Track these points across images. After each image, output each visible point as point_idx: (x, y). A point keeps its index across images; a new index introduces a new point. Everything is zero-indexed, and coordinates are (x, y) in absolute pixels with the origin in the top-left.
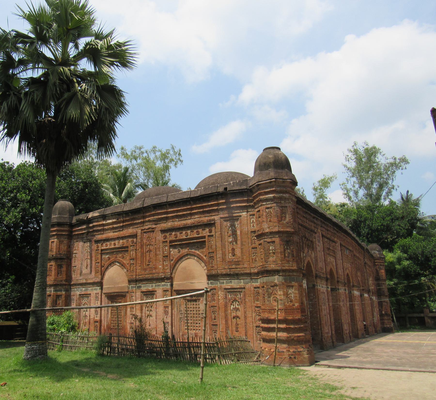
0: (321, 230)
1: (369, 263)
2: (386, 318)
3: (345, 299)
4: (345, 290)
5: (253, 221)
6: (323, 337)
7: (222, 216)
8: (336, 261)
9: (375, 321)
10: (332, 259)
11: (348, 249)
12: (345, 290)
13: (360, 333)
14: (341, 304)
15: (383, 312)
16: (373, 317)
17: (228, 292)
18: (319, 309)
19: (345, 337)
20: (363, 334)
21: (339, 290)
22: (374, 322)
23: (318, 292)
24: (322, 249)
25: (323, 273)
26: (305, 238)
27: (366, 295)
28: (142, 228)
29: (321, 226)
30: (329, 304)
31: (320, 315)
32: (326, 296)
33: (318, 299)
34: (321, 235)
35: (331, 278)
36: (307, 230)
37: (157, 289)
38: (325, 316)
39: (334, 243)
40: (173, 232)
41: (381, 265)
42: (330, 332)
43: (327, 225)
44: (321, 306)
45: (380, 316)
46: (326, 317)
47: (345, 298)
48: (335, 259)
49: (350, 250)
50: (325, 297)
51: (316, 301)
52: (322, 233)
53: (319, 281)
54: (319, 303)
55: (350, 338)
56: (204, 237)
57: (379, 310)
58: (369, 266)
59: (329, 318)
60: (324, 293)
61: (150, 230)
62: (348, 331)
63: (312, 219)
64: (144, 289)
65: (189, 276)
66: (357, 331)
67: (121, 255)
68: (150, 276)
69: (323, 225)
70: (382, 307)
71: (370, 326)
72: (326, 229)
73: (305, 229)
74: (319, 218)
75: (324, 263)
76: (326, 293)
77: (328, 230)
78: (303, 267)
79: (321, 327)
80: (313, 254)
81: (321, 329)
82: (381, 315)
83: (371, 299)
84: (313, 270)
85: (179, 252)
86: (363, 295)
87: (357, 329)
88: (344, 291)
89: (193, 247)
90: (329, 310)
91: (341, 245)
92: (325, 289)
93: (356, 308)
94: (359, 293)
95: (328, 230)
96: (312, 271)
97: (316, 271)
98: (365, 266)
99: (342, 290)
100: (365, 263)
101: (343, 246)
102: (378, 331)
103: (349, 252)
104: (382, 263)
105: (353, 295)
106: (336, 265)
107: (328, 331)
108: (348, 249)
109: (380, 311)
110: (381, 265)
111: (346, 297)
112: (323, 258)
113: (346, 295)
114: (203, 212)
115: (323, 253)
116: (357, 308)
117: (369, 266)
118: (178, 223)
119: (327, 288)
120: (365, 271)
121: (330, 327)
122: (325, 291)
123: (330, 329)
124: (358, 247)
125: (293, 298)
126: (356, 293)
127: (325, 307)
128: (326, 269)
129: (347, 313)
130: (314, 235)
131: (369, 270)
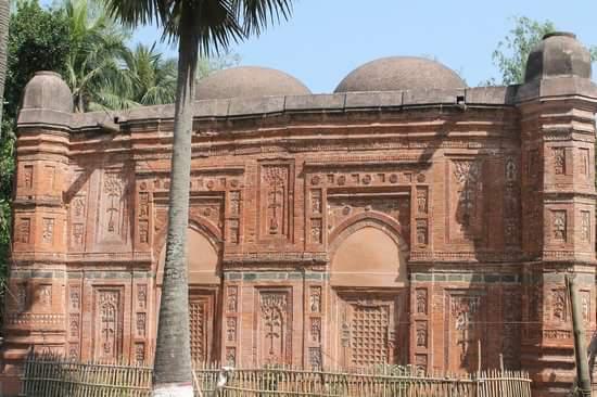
5: (511, 167)
7: (448, 151)
17: (452, 295)
28: (259, 156)
37: (292, 282)
40: (335, 172)
56: (409, 189)
61: (277, 162)
64: (262, 280)
65: (366, 261)
67: (204, 209)
68: (278, 258)
85: (346, 212)
89: (381, 206)
114: (346, 142)
118: (345, 156)
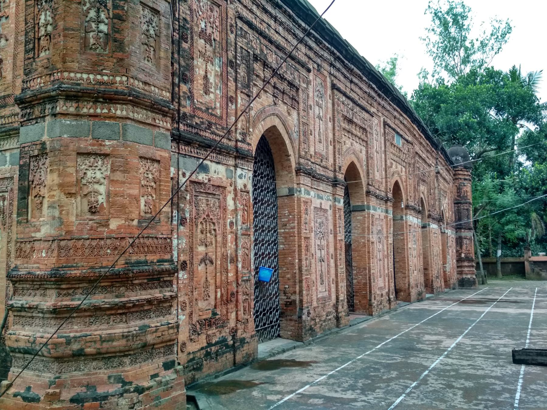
1: (444, 173)
2: (466, 264)
3: (385, 230)
4: (387, 212)
6: (305, 311)
8: (367, 152)
9: (448, 269)
10: (357, 146)
11: (401, 136)
12: (387, 212)
13: (414, 292)
14: (374, 238)
16: (444, 263)
18: (300, 246)
19: (375, 303)
20: (420, 294)
21: (369, 208)
22: (444, 272)
23: (299, 206)
24: (330, 115)
25: (326, 168)
26: (265, 65)
27: (434, 226)
29: (331, 65)
30: (335, 237)
31: (300, 260)
32: (330, 218)
33: (299, 223)
34: (329, 85)
35: (350, 182)
36: (274, 48)
38: (322, 260)
39: (366, 116)
41: (465, 179)
42: (334, 297)
43: (351, 71)
44: (307, 238)
45: (457, 261)
46: (324, 264)
47: (384, 226)
48: (367, 147)
49: (407, 141)
50: (327, 219)
51: (293, 228)
52: (332, 81)
53: (305, 180)
54: (299, 233)
55: (390, 304)
57: (457, 251)
58: (444, 179)
59: (332, 264)
60: (325, 211)
62: (387, 290)
63: (301, 35)
66: (409, 288)
69: (338, 65)
71: (437, 277)
72: (345, 77)
73: (263, 41)
74: (327, 44)
75: (331, 148)
76: (330, 212)
77: (351, 82)
78: (244, 134)
79: (301, 287)
80: (294, 114)
81: (301, 292)
82: (459, 260)
83: (443, 233)
84: (291, 152)
86: (429, 225)
87: (409, 285)
88: (384, 214)
90: (336, 249)
91: (385, 124)
92: (330, 203)
93: (409, 246)
94: (420, 220)
95: (351, 82)
96: (288, 156)
97: (300, 157)
98: (437, 177)
99: (378, 213)
100: (438, 173)
101: (390, 127)
102: (451, 286)
103: (403, 144)
104: (468, 175)
105: (406, 222)
106: (369, 158)
108: (401, 136)
109: (459, 253)
110: (465, 179)
111: (387, 225)
112: (331, 136)
113: (387, 221)
115: (330, 125)
116: (413, 248)
117: (444, 179)
119: (335, 200)
120: (436, 185)
121: (333, 286)
122: (328, 208)
123: (333, 290)
124: (425, 142)
125: (101, 199)
126: (413, 220)
127: (324, 243)
128: (335, 160)
129: (387, 256)
130: (303, 72)
131: (444, 185)
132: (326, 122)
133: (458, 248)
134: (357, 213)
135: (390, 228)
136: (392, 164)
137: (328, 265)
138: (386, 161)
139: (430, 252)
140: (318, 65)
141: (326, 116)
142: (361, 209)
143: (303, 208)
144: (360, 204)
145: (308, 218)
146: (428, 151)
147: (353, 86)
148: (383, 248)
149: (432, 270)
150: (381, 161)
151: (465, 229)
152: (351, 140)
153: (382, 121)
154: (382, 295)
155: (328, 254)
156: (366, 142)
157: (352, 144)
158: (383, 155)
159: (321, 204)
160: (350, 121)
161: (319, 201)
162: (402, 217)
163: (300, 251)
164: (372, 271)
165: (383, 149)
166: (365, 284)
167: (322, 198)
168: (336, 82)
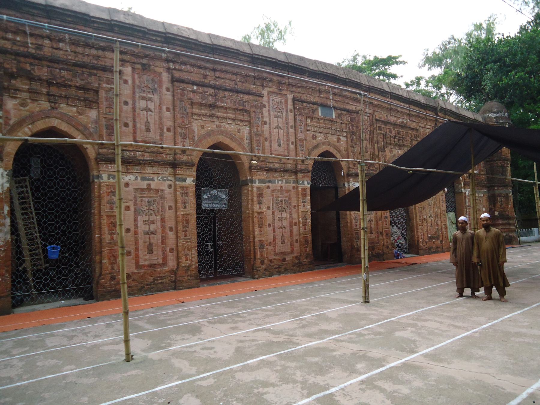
0: (168, 70)
2: (501, 222)
10: (231, 127)
15: (496, 213)
18: (100, 223)
21: (252, 181)
48: (250, 127)
70: (494, 205)
91: (294, 100)
107: (160, 261)
122: (166, 187)
132: (160, 112)
133: (492, 207)
134: (244, 188)
135: (305, 195)
136: (314, 137)
137: (162, 237)
138: (296, 135)
139: (416, 214)
140: (143, 65)
141: (160, 108)
142: (246, 183)
143: (104, 189)
144: (245, 179)
145: (116, 199)
146: (410, 115)
147: (217, 74)
148: (291, 217)
149: (417, 232)
150: (288, 136)
151: (498, 186)
152: (218, 123)
153: (290, 97)
154: (284, 260)
155: (163, 226)
156: (249, 122)
157: (218, 127)
158: (292, 131)
159: (149, 185)
160: (213, 106)
161: (146, 182)
162: (344, 185)
163: (100, 228)
164: (257, 239)
165: (291, 123)
166: (250, 250)
167: (153, 180)
168: (177, 74)
